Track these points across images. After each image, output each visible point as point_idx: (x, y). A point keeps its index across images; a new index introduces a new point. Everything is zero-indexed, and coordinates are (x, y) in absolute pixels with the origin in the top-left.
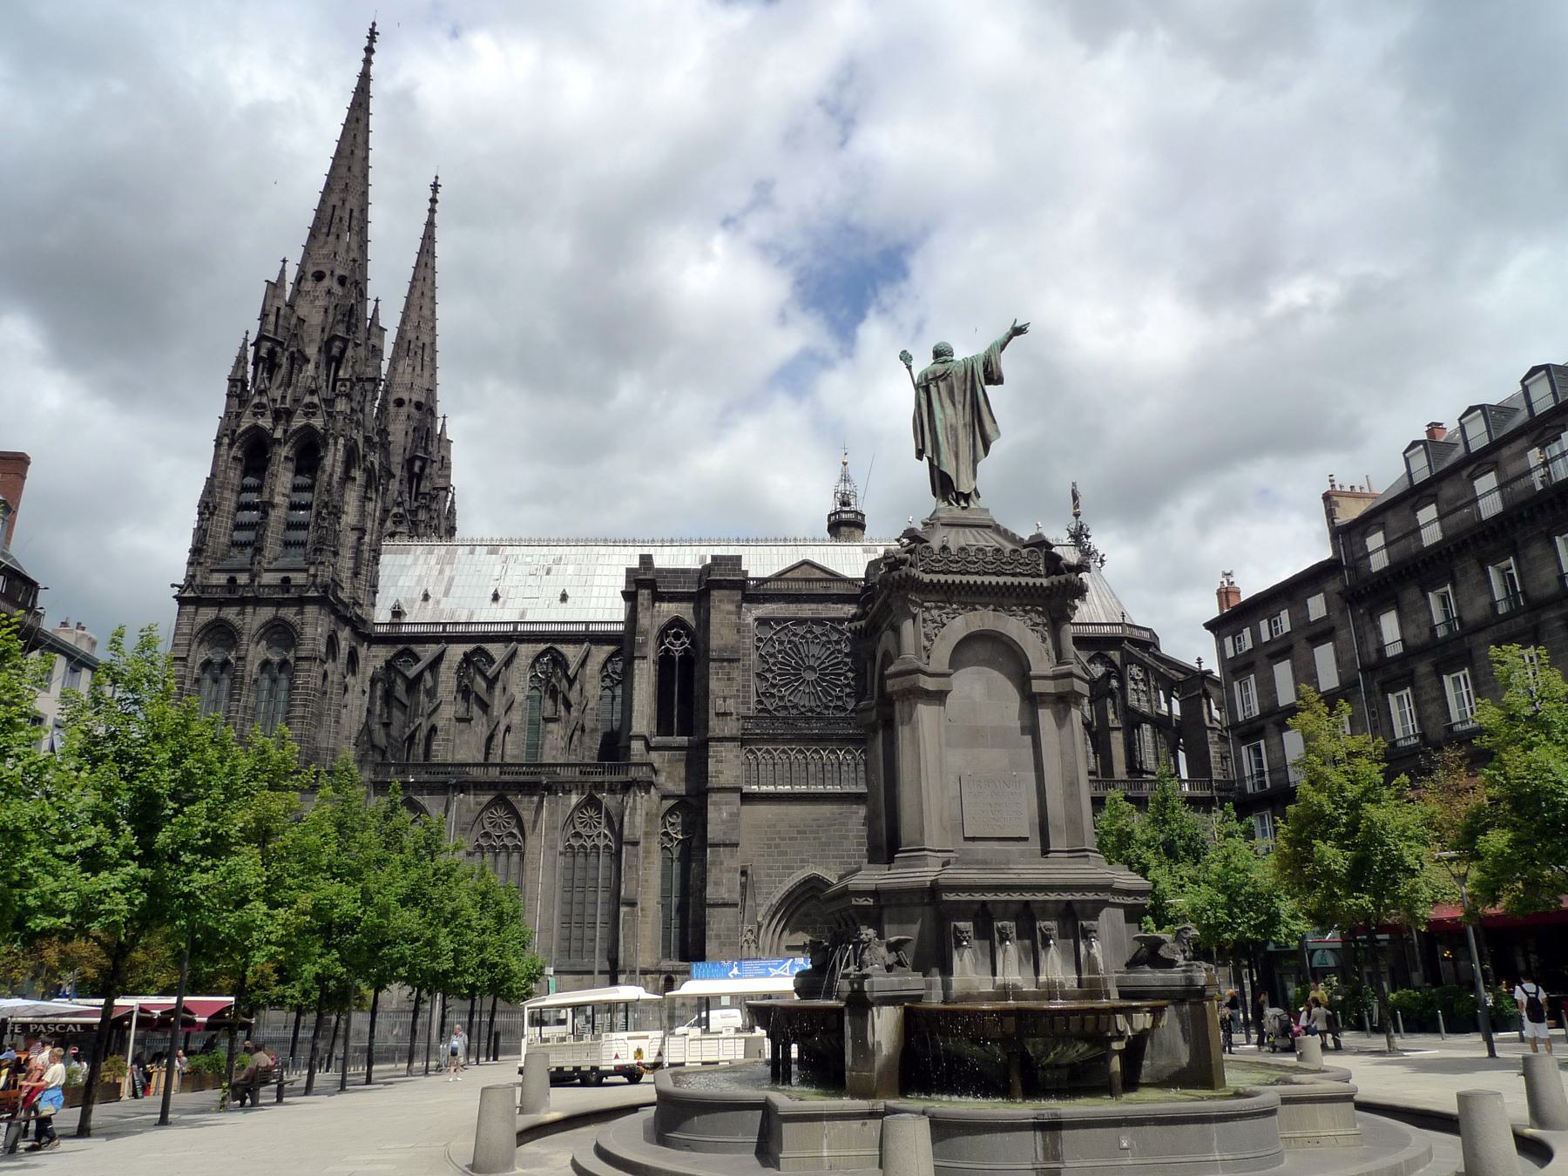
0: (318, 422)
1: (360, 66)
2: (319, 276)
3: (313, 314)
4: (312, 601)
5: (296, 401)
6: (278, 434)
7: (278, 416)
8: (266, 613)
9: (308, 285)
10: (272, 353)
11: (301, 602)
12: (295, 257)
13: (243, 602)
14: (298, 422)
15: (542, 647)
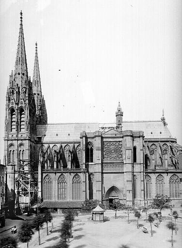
0: (24, 105)
1: (20, 22)
2: (19, 74)
3: (19, 81)
4: (27, 139)
5: (18, 101)
6: (17, 108)
7: (16, 104)
8: (20, 142)
9: (17, 75)
10: (13, 91)
11: (25, 140)
12: (14, 69)
13: (15, 140)
14: (20, 105)
15: (66, 144)
